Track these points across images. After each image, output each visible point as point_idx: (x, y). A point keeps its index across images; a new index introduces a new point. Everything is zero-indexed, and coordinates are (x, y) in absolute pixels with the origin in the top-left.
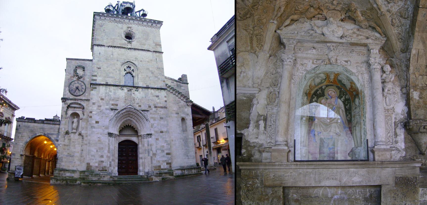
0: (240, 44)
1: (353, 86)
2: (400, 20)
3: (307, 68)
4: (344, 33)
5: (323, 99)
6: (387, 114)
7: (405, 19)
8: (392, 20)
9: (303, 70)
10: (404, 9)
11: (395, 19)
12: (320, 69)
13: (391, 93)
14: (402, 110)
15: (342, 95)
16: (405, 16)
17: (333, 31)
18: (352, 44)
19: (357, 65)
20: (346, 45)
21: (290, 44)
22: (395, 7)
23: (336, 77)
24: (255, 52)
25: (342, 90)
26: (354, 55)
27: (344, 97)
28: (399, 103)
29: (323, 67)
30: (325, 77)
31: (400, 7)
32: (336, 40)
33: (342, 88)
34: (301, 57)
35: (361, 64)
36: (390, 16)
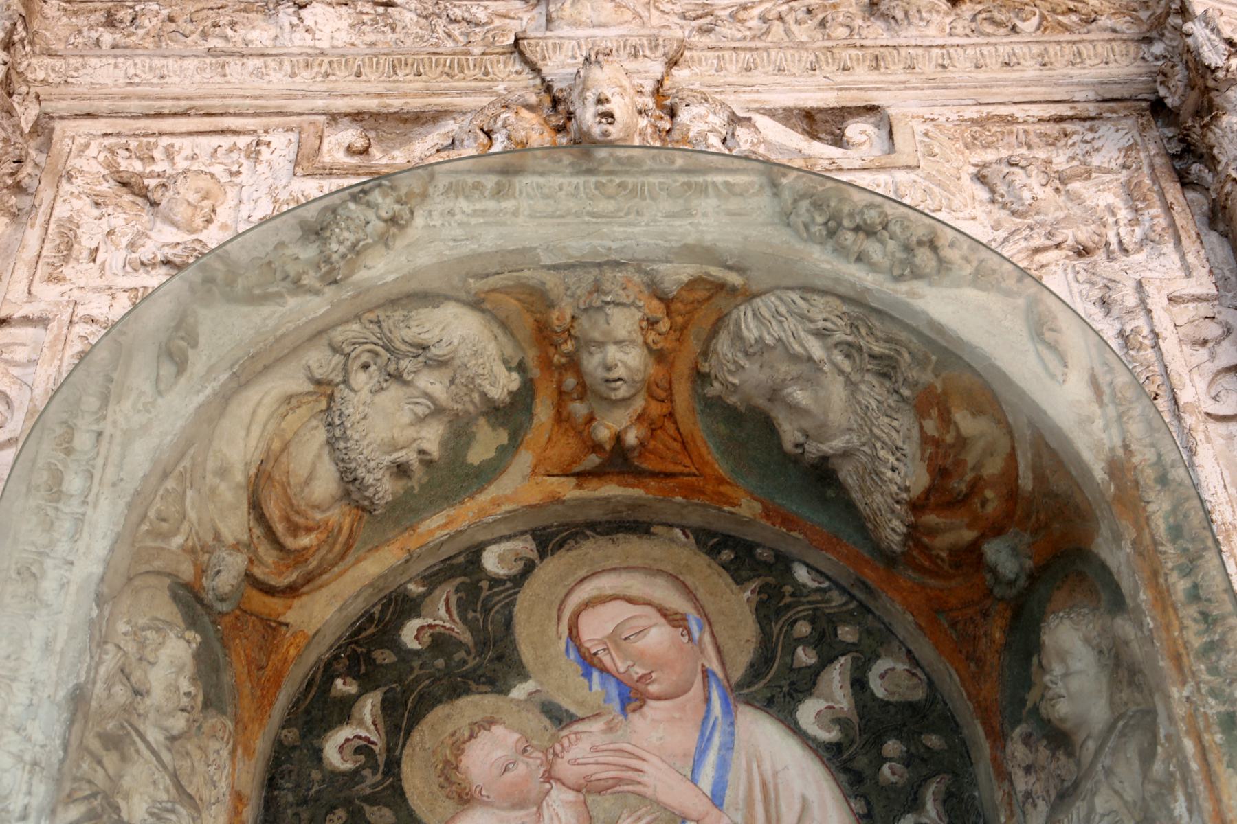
1: (962, 442)
5: (489, 723)
15: (805, 657)
23: (683, 367)
25: (800, 591)
27: (836, 679)
30: (513, 382)
33: (795, 541)
34: (134, 106)
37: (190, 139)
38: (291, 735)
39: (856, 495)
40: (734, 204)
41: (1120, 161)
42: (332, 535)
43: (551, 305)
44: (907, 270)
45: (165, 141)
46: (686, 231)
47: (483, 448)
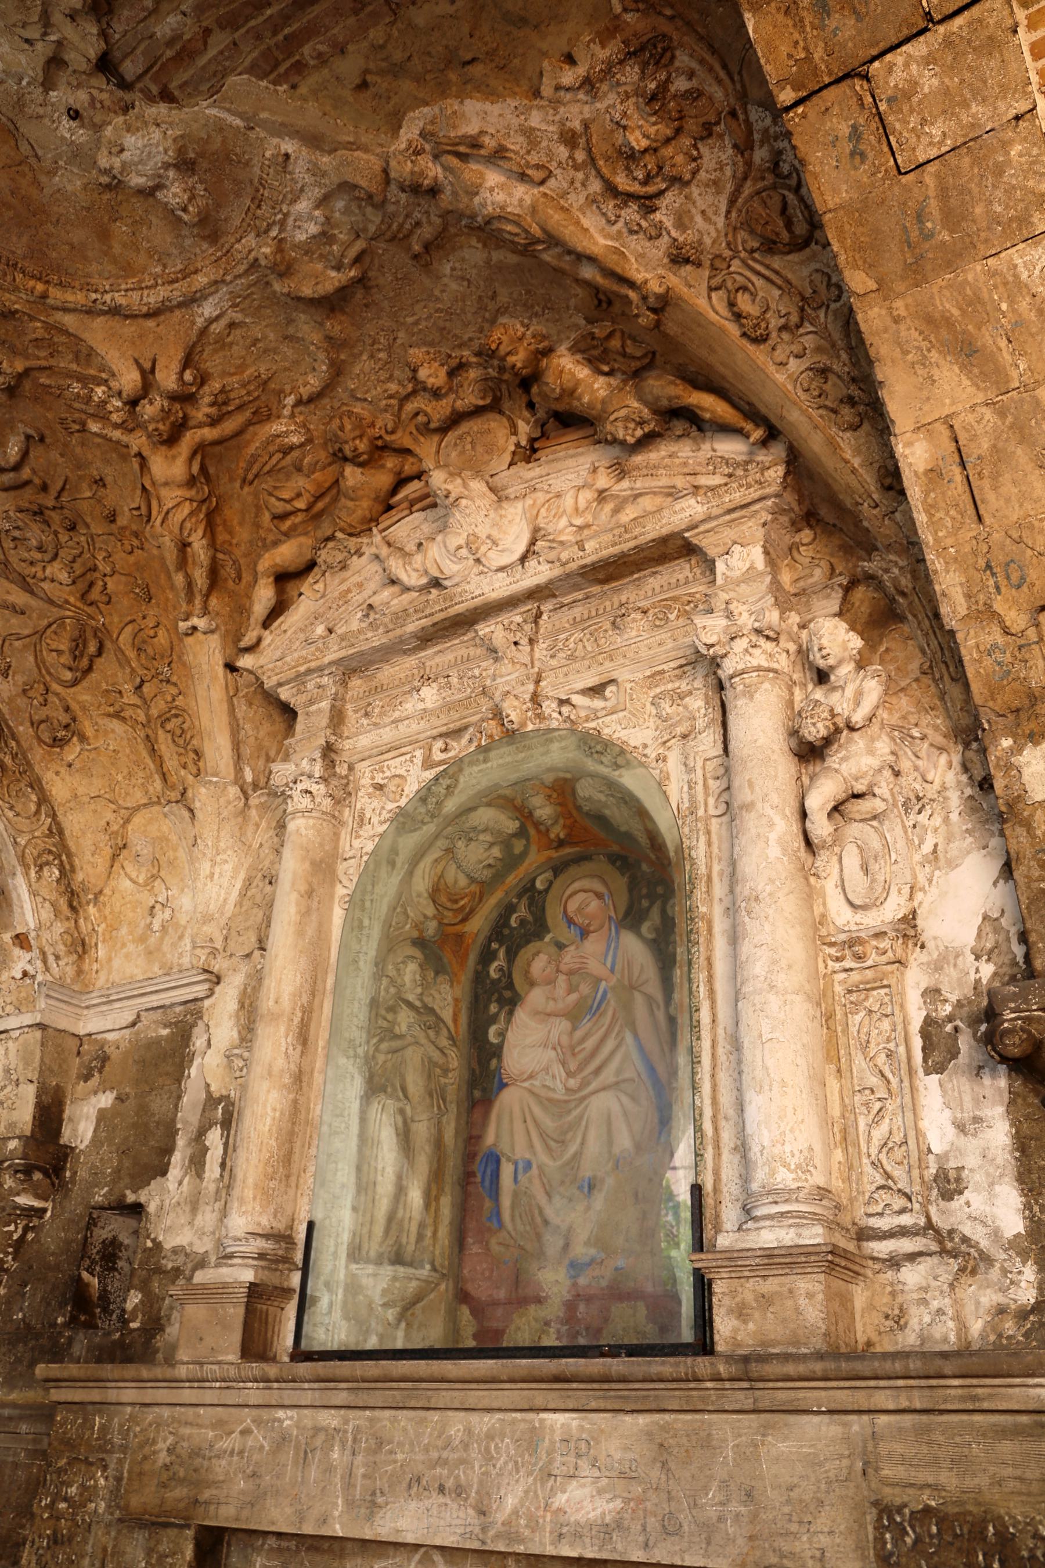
0: (120, 778)
2: (777, 273)
4: (536, 530)
6: (855, 976)
7: (807, 251)
8: (732, 304)
10: (760, 185)
11: (744, 289)
12: (461, 785)
13: (878, 805)
14: (986, 917)
16: (789, 225)
17: (471, 544)
18: (601, 576)
19: (652, 693)
20: (579, 595)
21: (311, 702)
22: (701, 204)
24: (183, 794)
26: (634, 633)
28: (952, 865)
29: (476, 769)
31: (729, 187)
32: (499, 587)
36: (711, 289)
38: (480, 968)
40: (563, 744)
42: (473, 895)
43: (513, 800)
44: (617, 766)
46: (548, 761)
47: (519, 846)
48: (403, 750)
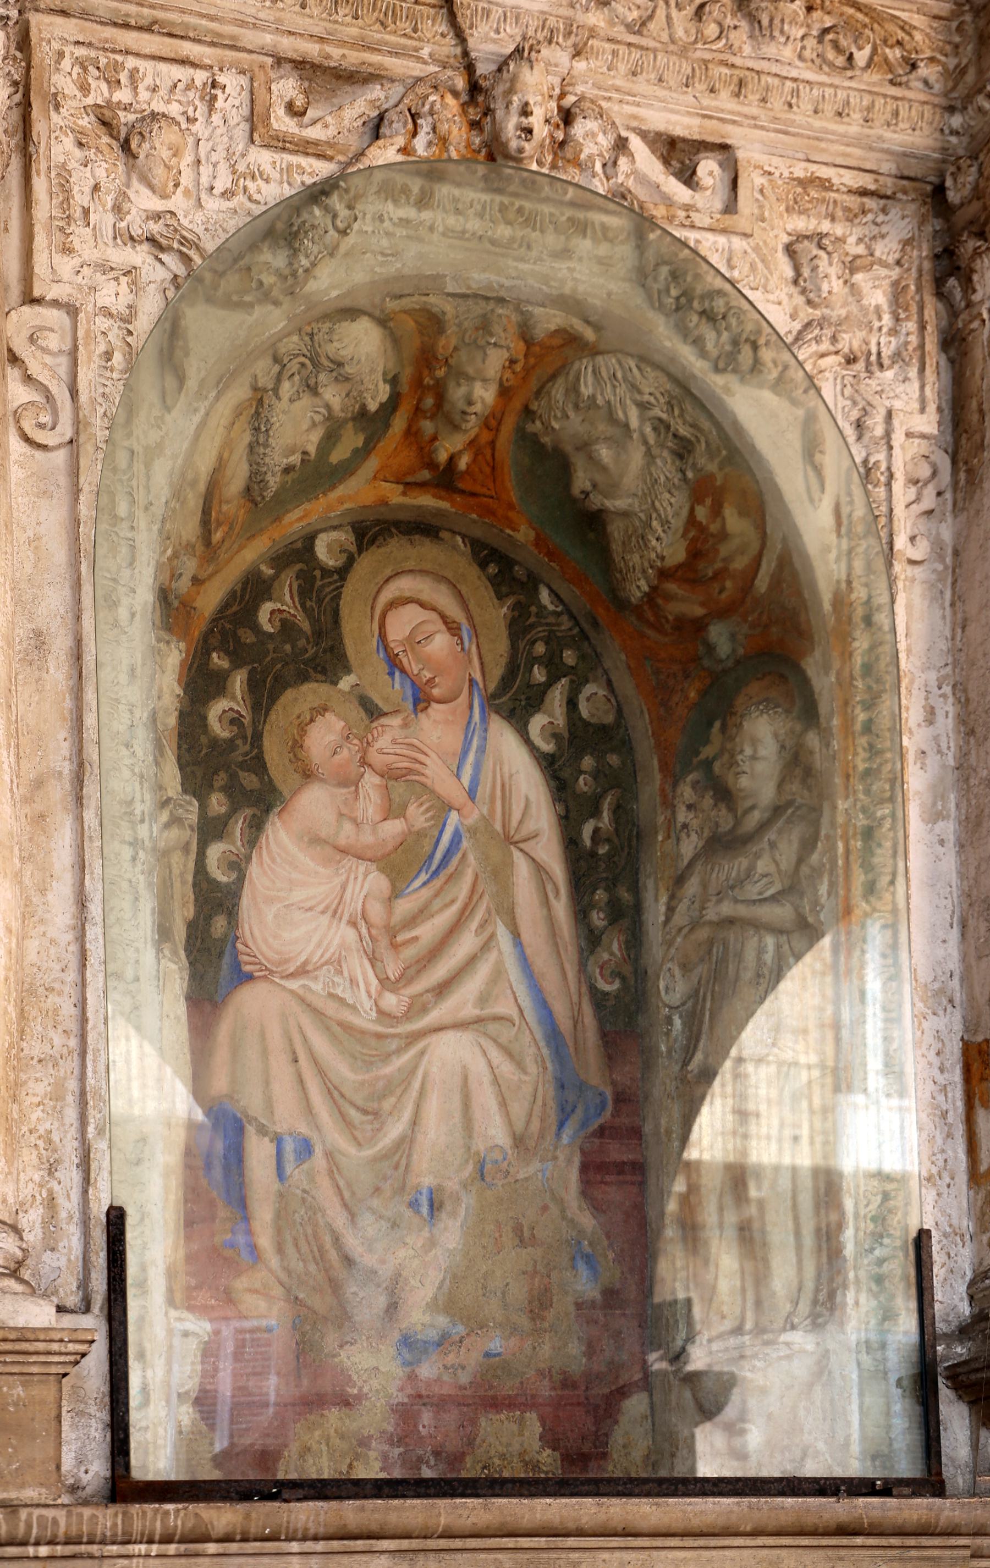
3: (178, 202)
9: (135, 222)
35: (851, 217)
37: (152, 63)
39: (616, 547)
41: (897, 256)
45: (131, 62)
48: (188, 49)
